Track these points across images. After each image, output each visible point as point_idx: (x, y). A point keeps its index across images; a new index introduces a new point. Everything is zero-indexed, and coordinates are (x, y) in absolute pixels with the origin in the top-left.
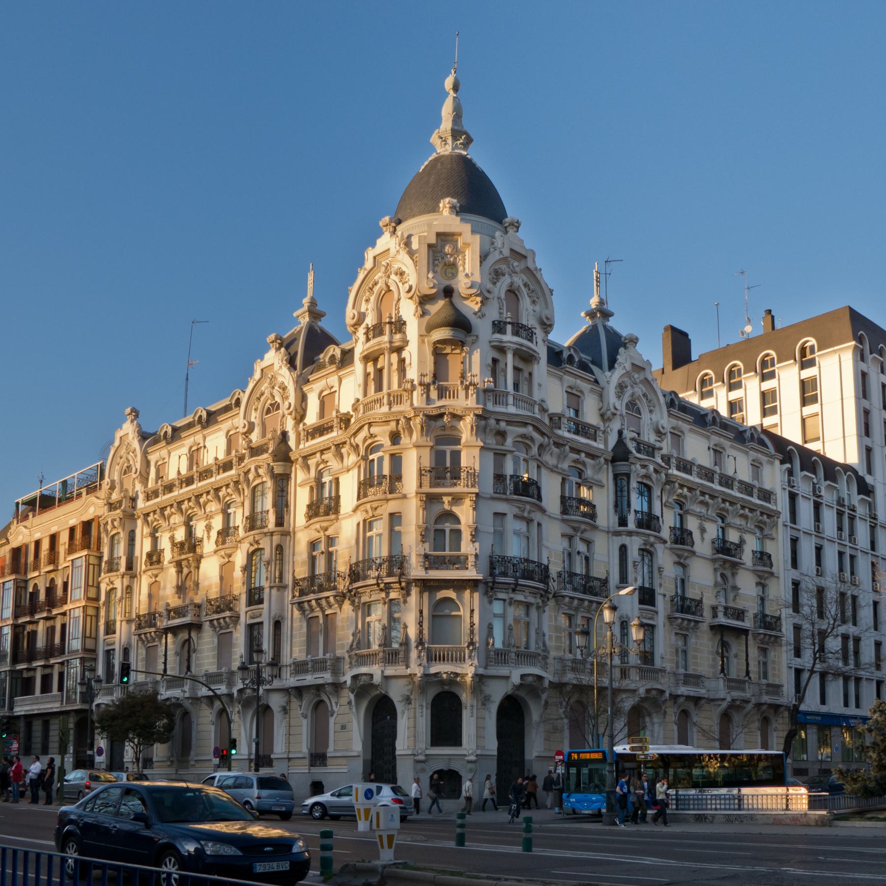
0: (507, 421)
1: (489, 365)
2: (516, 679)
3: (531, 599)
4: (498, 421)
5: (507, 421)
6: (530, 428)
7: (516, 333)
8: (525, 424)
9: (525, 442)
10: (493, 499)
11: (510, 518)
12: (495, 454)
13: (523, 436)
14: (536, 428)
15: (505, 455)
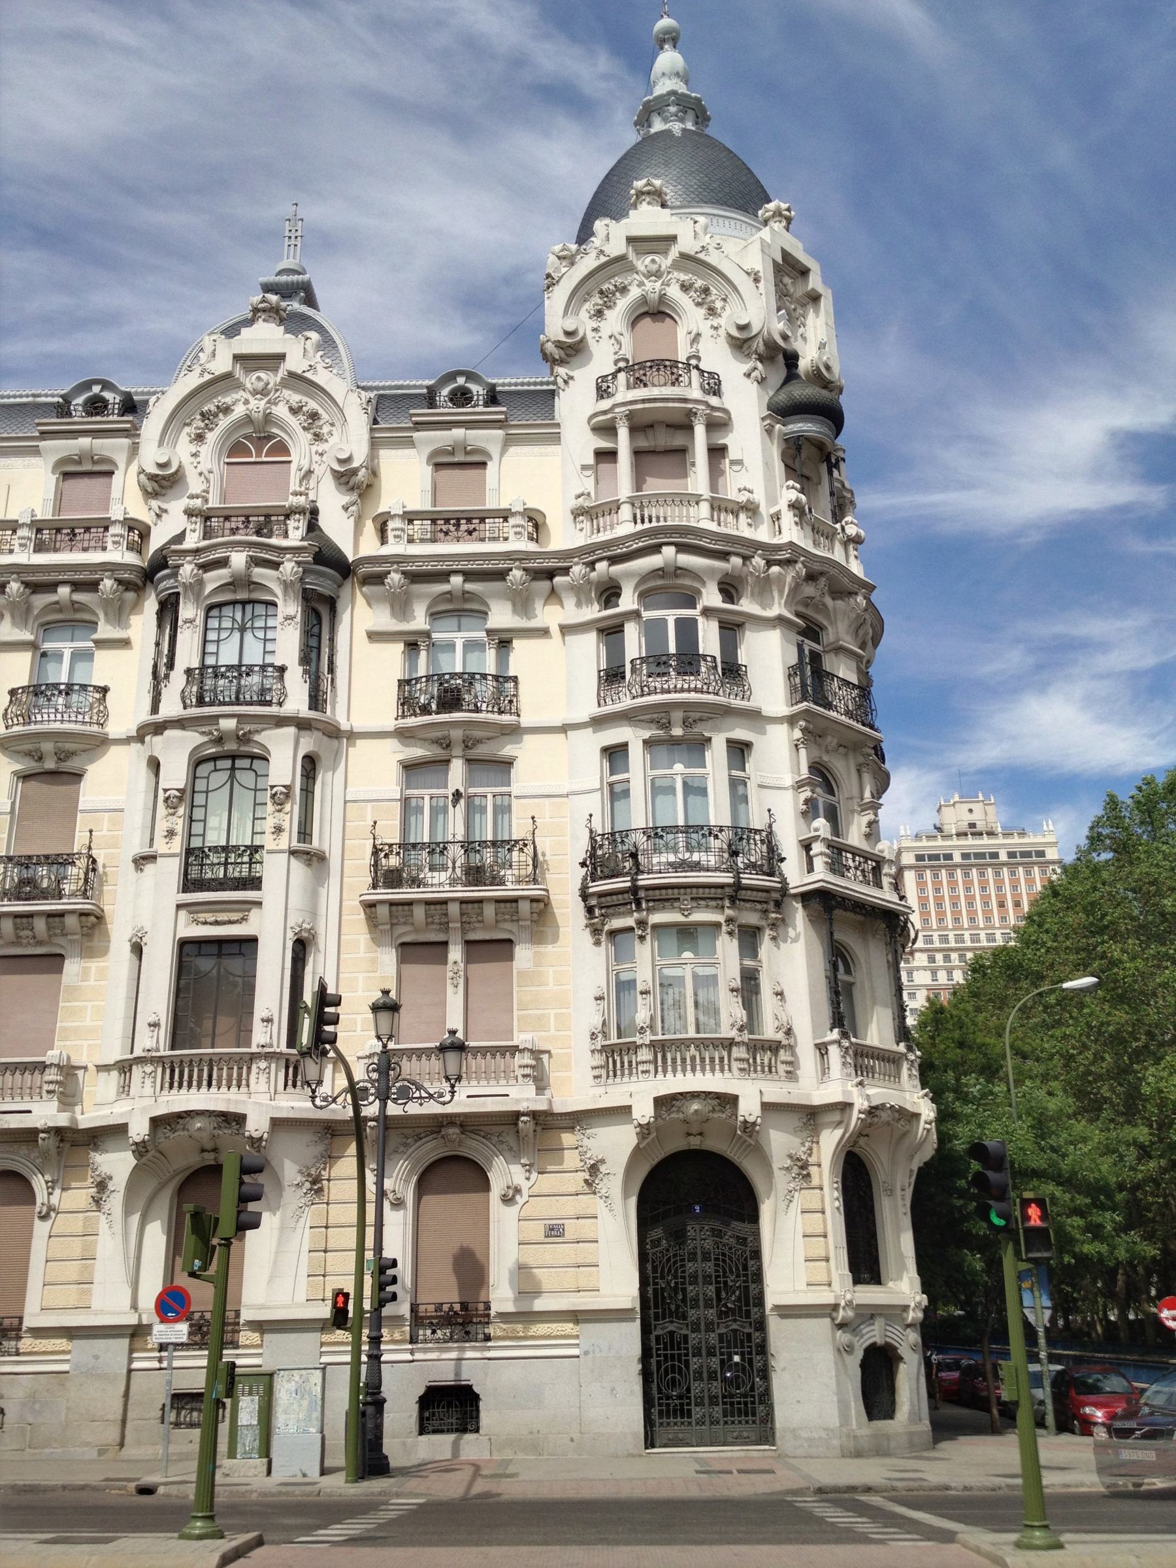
0: (609, 558)
1: (584, 467)
2: (644, 1111)
3: (701, 916)
4: (592, 565)
5: (609, 558)
6: (668, 551)
7: (640, 382)
8: (656, 549)
9: (670, 588)
10: (598, 722)
11: (636, 753)
12: (601, 631)
13: (659, 573)
14: (682, 548)
15: (623, 626)
